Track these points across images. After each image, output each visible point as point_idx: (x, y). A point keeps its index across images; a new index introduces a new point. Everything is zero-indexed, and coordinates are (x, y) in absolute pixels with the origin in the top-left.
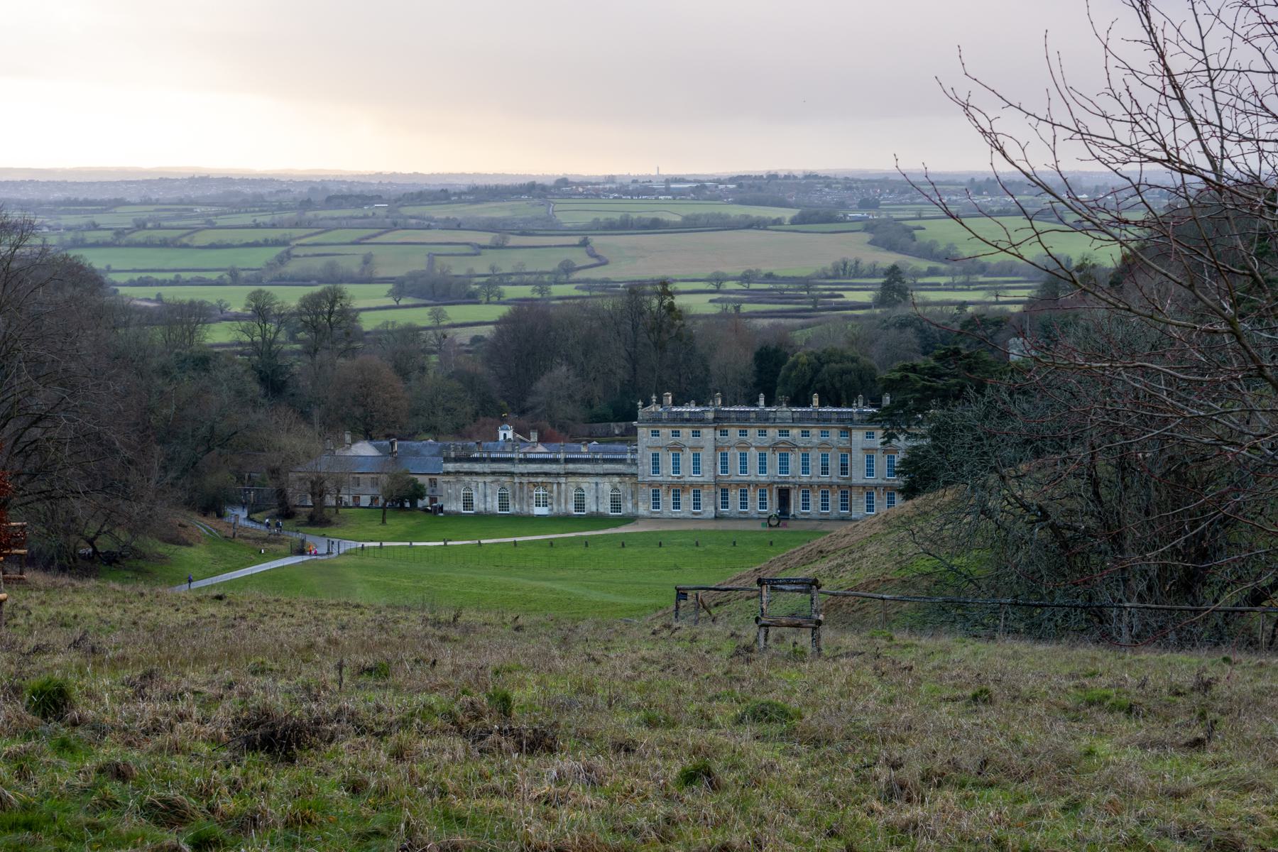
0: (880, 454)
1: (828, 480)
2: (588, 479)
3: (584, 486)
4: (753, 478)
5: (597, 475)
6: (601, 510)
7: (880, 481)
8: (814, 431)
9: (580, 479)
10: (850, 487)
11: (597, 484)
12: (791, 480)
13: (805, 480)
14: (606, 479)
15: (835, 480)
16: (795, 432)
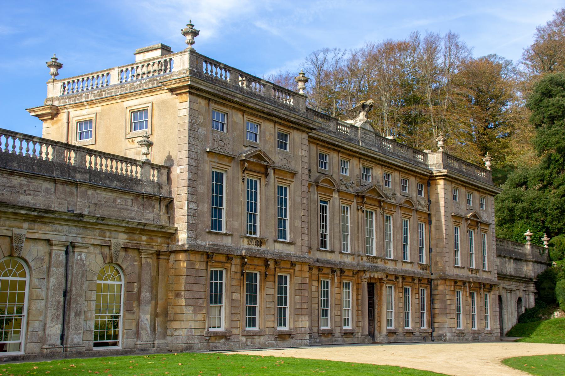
0: (464, 225)
1: (408, 267)
2: (44, 231)
3: (33, 252)
4: (335, 258)
5: (78, 219)
6: (75, 338)
7: (464, 273)
8: (396, 176)
9: (24, 229)
10: (430, 281)
11: (70, 248)
12: (380, 264)
13: (390, 266)
14: (93, 237)
15: (417, 269)
16: (377, 172)
